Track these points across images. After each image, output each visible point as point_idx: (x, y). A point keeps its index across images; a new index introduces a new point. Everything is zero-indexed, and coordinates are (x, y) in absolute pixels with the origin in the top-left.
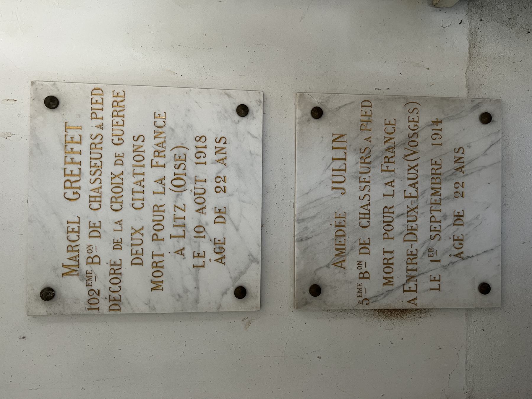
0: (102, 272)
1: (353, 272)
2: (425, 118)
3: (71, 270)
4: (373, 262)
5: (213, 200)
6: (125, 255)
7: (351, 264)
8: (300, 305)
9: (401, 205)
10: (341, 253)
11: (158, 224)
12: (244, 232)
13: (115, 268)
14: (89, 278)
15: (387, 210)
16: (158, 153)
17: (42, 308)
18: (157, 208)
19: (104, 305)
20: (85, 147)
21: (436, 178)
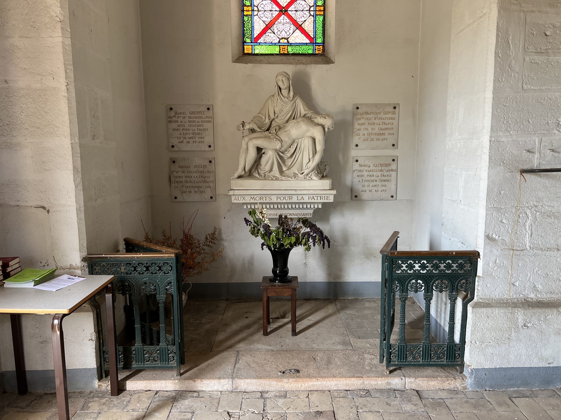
0: (176, 119)
1: (178, 170)
2: (211, 185)
3: (176, 113)
4: (180, 174)
5: (191, 140)
6: (179, 123)
7: (180, 169)
8: (171, 159)
9: (192, 179)
10: (182, 167)
11: (186, 130)
12: (185, 147)
13: (177, 122)
14: (175, 116)
15: (191, 177)
16: (200, 129)
17: (169, 108)
18: (189, 130)
19: (169, 120)
20: (200, 115)
21: (198, 187)
